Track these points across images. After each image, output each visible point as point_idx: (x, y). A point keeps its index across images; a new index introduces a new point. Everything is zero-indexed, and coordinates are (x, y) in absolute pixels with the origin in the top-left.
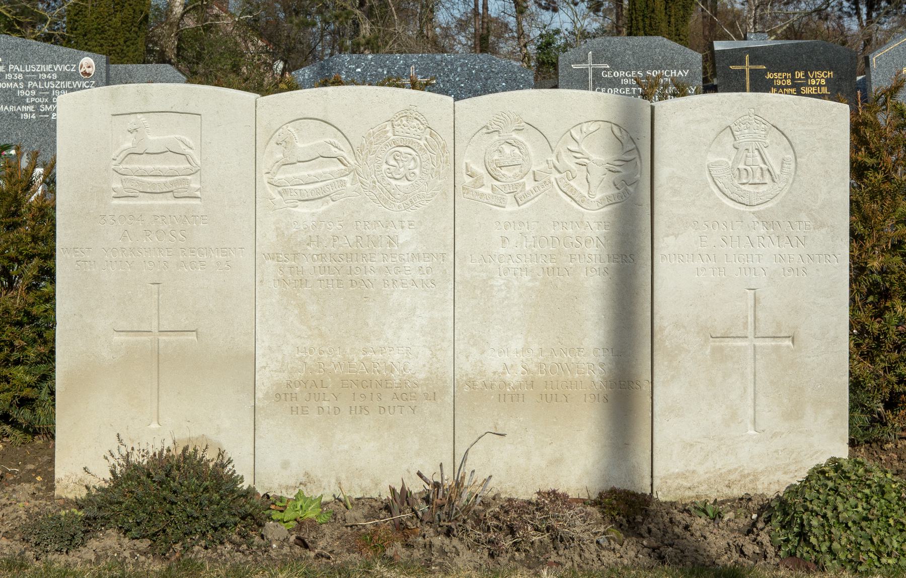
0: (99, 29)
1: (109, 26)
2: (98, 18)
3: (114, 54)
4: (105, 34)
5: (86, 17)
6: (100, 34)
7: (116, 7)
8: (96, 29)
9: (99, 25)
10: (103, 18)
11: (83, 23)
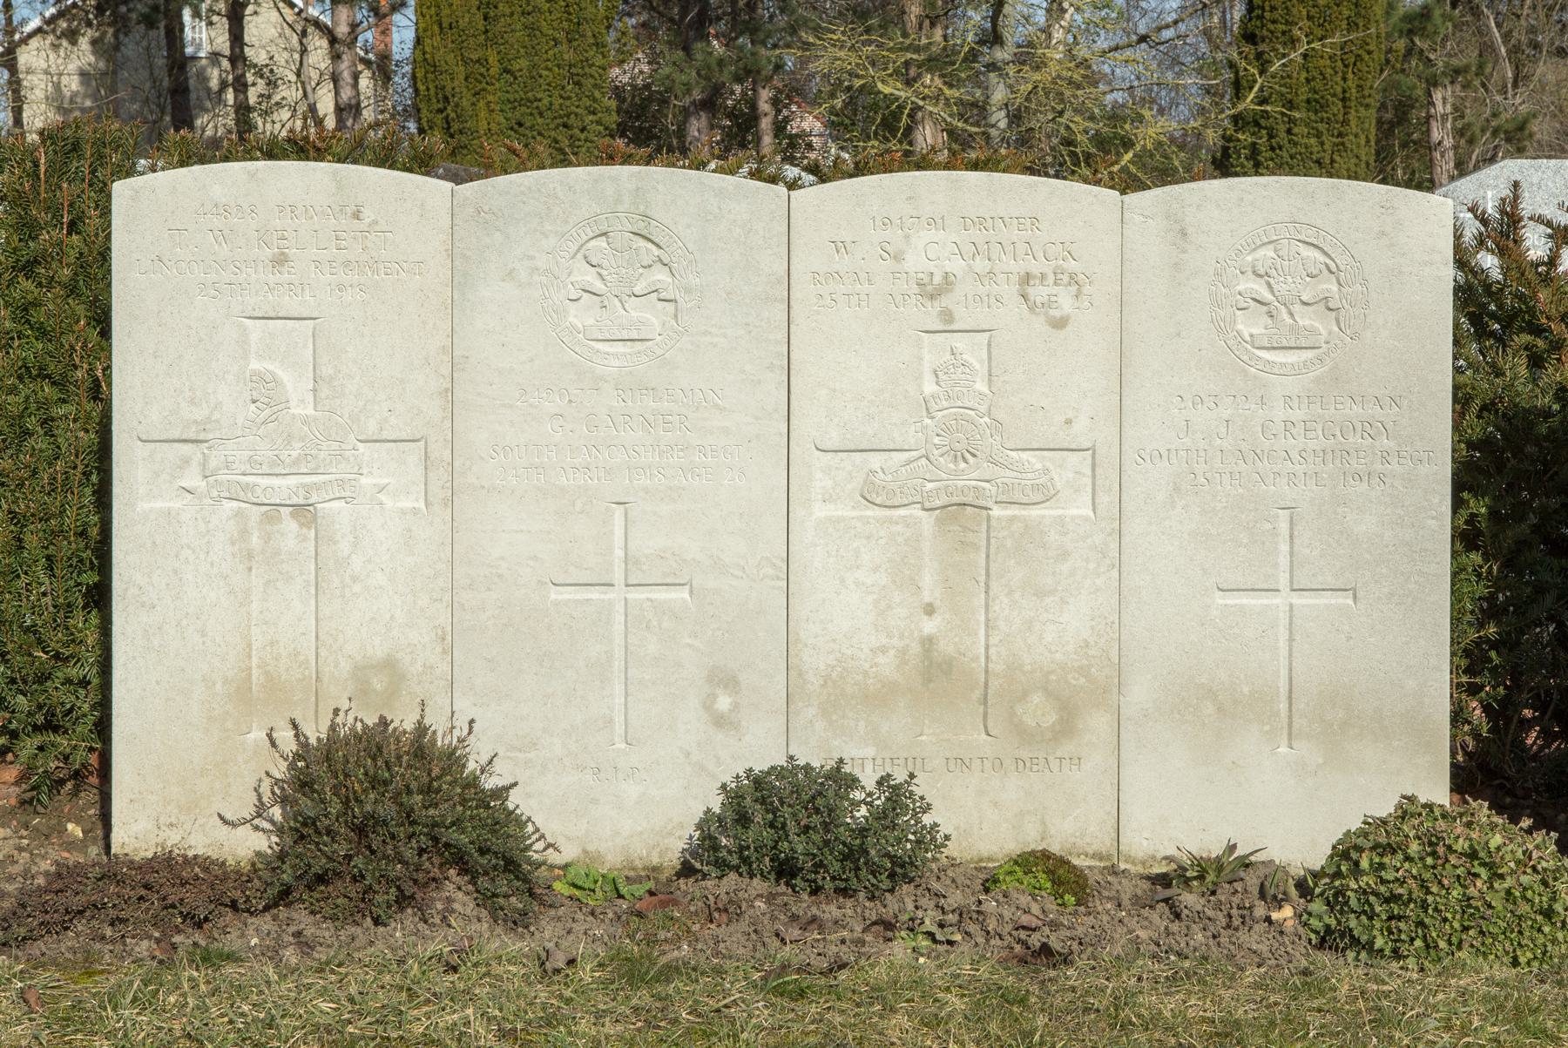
0: (1317, 101)
1: (1334, 95)
2: (1314, 79)
3: (1338, 151)
4: (1326, 112)
5: (1289, 77)
6: (1316, 112)
7: (1345, 57)
8: (1308, 101)
9: (1316, 92)
10: (1324, 78)
11: (1283, 89)
